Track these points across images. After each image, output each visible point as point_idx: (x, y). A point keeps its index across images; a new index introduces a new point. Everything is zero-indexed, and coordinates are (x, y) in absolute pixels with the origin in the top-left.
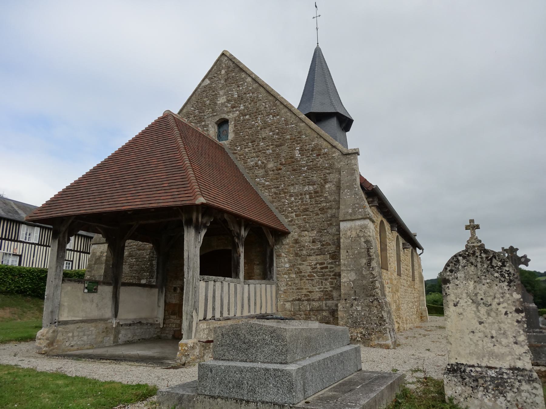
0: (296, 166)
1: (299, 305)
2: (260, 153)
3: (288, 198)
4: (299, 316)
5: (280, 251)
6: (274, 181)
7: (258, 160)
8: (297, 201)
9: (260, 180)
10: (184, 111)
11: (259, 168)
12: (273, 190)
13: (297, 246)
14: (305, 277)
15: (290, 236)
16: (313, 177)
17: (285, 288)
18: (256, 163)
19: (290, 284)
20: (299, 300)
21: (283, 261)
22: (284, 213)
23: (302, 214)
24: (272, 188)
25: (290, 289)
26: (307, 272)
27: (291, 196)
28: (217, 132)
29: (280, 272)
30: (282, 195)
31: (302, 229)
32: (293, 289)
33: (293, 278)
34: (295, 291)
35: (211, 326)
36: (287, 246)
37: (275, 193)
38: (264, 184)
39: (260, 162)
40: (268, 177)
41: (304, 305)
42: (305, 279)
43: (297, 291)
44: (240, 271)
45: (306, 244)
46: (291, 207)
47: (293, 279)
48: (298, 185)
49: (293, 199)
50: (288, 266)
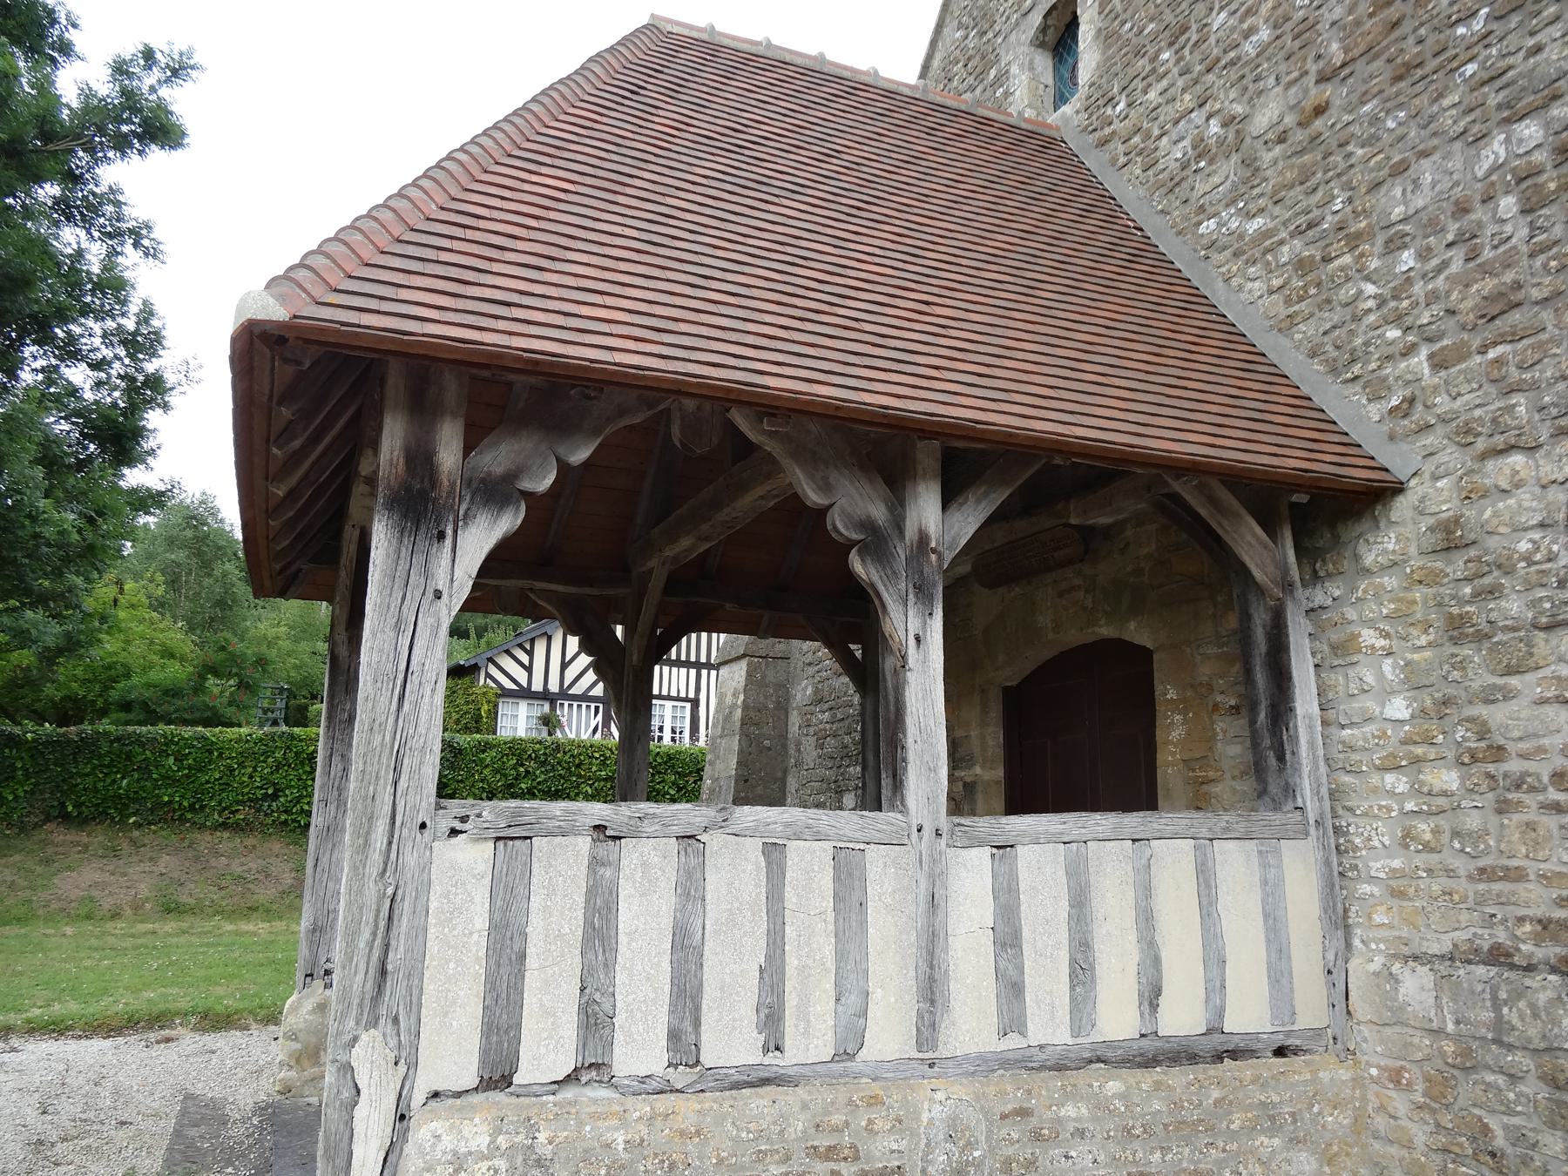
0: (1411, 40)
1: (1494, 998)
2: (1211, 77)
3: (1374, 264)
4: (1501, 1080)
5: (1351, 614)
6: (1292, 193)
7: (1208, 119)
8: (1435, 262)
9: (1220, 225)
10: (936, 63)
11: (1211, 162)
12: (1285, 254)
13: (1457, 566)
14: (1533, 789)
15: (1402, 507)
16: (1538, 49)
17: (1397, 863)
18: (1198, 142)
19: (1428, 836)
20: (1498, 956)
21: (1370, 679)
22: (1357, 369)
23: (1476, 343)
24: (1282, 243)
25: (1429, 871)
26: (1541, 750)
27: (1394, 245)
28: (1050, 82)
29: (1355, 757)
30: (1337, 263)
31: (1481, 444)
32: (1450, 873)
33: (1445, 794)
34: (1462, 885)
35: (542, 1137)
36: (1390, 581)
37: (1302, 266)
38: (1241, 237)
39: (1214, 127)
40: (1256, 191)
41: (1532, 1006)
42: (1531, 801)
43: (1482, 887)
44: (904, 760)
45: (1524, 546)
46: (1397, 319)
47: (1442, 801)
48: (1436, 157)
49: (1407, 259)
50: (1406, 714)
